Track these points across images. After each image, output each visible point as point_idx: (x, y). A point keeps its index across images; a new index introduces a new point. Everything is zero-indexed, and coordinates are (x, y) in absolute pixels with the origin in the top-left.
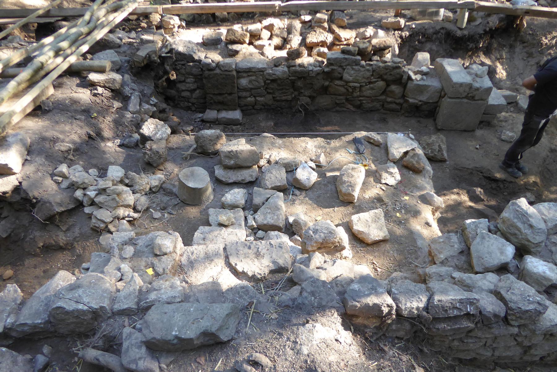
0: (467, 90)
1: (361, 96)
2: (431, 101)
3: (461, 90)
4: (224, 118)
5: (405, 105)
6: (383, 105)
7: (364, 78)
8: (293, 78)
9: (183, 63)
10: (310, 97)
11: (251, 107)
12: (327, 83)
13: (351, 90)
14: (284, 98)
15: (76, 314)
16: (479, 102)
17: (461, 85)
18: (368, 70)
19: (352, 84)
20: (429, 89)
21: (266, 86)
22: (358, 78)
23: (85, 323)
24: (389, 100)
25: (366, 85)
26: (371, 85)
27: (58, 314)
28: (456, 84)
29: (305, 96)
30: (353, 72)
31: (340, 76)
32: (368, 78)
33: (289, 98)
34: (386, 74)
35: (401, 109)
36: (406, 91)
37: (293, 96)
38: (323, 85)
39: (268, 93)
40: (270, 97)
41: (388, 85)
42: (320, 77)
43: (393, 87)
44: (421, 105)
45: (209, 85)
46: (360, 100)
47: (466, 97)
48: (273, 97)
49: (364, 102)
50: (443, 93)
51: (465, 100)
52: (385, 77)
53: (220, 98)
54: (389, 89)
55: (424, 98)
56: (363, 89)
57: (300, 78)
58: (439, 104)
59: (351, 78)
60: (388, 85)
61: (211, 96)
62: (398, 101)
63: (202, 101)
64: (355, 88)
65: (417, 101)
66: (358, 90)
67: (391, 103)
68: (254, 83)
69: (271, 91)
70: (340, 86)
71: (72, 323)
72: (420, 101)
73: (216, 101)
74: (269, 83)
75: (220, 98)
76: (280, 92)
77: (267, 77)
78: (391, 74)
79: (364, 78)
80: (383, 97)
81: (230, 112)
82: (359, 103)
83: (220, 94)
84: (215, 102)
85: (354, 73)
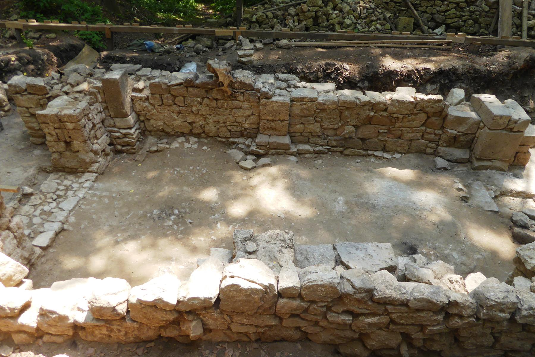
1: (402, 127)
2: (469, 132)
3: (501, 122)
4: (275, 142)
5: (444, 136)
7: (407, 110)
8: (341, 108)
9: (242, 91)
10: (354, 126)
11: (299, 134)
12: (372, 114)
13: (394, 121)
14: (331, 126)
15: (249, 292)
16: (517, 133)
19: (395, 115)
21: (316, 115)
22: (401, 109)
23: (253, 302)
24: (429, 130)
25: (409, 116)
27: (230, 291)
28: (496, 116)
29: (351, 125)
31: (385, 107)
32: (410, 111)
33: (336, 126)
34: (428, 107)
35: (439, 139)
36: (445, 123)
37: (340, 124)
38: (369, 115)
39: (316, 121)
40: (318, 125)
41: (428, 118)
43: (433, 119)
44: (460, 135)
45: (265, 112)
48: (321, 126)
49: (405, 132)
50: (482, 124)
51: (504, 132)
52: (427, 110)
53: (273, 124)
54: (429, 120)
55: (463, 129)
56: (406, 120)
57: (347, 109)
58: (477, 135)
60: (428, 118)
61: (265, 121)
62: (436, 132)
63: (254, 126)
66: (400, 120)
67: (430, 133)
68: (305, 111)
69: (320, 119)
70: (385, 116)
71: (240, 301)
73: (269, 127)
74: (318, 113)
75: (273, 124)
76: (328, 121)
77: (318, 107)
78: (433, 107)
79: (407, 110)
80: (424, 128)
81: (281, 137)
82: (400, 132)
83: (273, 121)
84: (268, 128)
85: (398, 105)
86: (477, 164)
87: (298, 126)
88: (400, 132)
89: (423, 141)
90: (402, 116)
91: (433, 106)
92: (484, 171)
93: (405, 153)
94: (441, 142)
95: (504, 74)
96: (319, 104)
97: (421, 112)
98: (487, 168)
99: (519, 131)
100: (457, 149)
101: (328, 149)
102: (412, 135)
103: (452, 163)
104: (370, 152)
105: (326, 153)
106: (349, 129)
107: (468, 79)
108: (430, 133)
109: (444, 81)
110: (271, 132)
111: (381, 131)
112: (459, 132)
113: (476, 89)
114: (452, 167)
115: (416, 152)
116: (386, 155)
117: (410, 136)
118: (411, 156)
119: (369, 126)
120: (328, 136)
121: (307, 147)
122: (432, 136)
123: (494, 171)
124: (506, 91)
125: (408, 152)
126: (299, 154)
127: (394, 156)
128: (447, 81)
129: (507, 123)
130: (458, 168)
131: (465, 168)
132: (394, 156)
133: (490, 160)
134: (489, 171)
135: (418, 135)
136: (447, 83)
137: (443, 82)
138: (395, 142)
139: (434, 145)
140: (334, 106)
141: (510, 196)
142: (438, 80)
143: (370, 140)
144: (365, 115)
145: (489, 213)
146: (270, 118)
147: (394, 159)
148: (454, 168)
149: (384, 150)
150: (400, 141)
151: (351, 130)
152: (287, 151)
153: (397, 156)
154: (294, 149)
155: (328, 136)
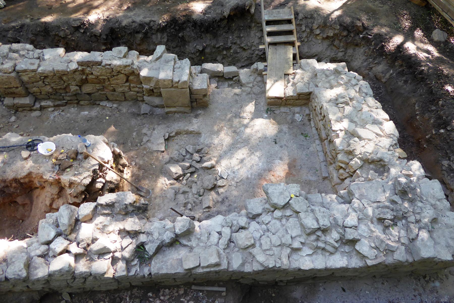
0: (170, 82)
3: (166, 83)
6: (130, 89)
18: (108, 68)
20: (154, 79)
26: (116, 77)
30: (98, 70)
32: (110, 73)
33: (62, 87)
34: (122, 70)
40: (48, 87)
42: (77, 73)
51: (173, 89)
53: (11, 90)
59: (99, 74)
62: (138, 86)
64: (104, 79)
66: (107, 80)
67: (134, 87)
81: (23, 99)
82: (112, 88)
87: (34, 89)
89: (132, 93)
90: (106, 78)
94: (145, 93)
95: (217, 21)
96: (40, 73)
101: (66, 103)
102: (122, 89)
105: (65, 105)
106: (73, 88)
108: (134, 87)
110: (14, 96)
111: (98, 88)
115: (132, 100)
116: (108, 104)
117: (121, 89)
119: (87, 84)
120: (61, 94)
121: (49, 103)
122: (137, 89)
124: (224, 34)
126: (42, 108)
133: (175, 107)
135: (126, 89)
138: (112, 95)
139: (141, 95)
140: (52, 74)
143: (94, 94)
144: (78, 78)
146: (6, 87)
149: (108, 99)
150: (116, 93)
151: (75, 89)
152: (32, 108)
154: (37, 106)
155: (61, 94)
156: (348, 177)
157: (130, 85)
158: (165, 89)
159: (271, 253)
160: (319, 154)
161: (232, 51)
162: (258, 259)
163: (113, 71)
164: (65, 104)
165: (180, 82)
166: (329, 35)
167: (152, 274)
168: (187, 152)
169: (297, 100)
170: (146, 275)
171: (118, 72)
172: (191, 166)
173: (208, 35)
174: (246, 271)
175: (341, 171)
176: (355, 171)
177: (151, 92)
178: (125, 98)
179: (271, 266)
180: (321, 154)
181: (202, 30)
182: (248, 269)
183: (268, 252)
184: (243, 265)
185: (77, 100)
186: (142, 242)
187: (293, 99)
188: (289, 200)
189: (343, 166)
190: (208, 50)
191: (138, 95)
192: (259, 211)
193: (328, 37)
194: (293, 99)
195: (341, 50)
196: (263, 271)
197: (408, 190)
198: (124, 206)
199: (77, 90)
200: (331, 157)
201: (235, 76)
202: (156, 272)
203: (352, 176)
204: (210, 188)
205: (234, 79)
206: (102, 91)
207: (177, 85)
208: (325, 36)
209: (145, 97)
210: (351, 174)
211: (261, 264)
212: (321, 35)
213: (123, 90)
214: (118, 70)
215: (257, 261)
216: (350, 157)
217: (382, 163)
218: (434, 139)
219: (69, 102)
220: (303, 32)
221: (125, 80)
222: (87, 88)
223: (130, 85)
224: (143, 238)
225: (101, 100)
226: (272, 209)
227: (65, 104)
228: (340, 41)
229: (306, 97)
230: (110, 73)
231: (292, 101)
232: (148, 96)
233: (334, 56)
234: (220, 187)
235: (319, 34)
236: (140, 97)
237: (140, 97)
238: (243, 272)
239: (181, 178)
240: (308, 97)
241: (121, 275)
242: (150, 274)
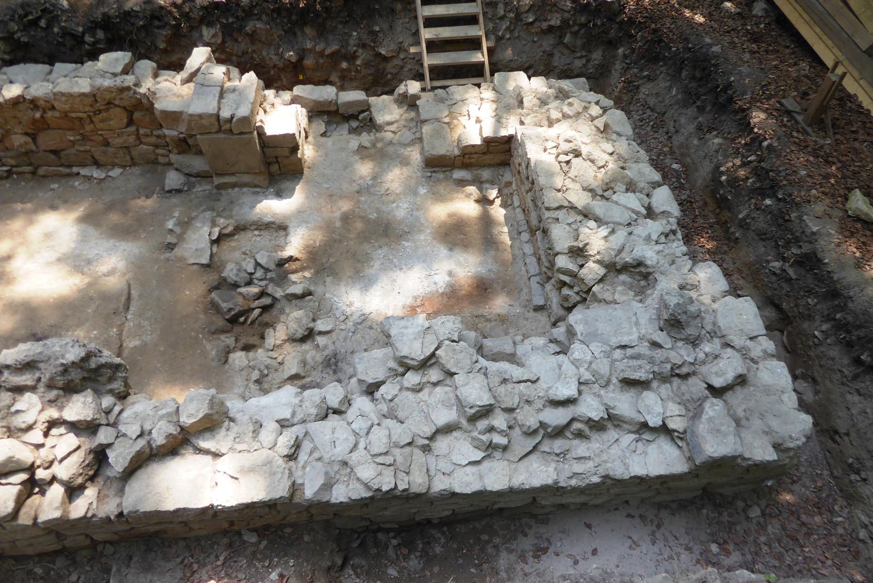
0: (213, 120)
16: (243, 136)
17: (200, 116)
42: (22, 107)
46: (101, 135)
47: (219, 131)
51: (222, 136)
59: (67, 107)
62: (155, 133)
64: (80, 119)
65: (176, 133)
66: (88, 121)
67: (147, 136)
72: (182, 133)
78: (121, 99)
80: (132, 129)
86: (217, 181)
88: (101, 138)
89: (145, 147)
90: (85, 115)
91: (122, 96)
92: (230, 190)
93: (130, 166)
97: (111, 106)
98: (234, 185)
99: (242, 133)
100: (196, 156)
103: (193, 179)
104: (75, 170)
107: (267, 15)
108: (147, 136)
109: (227, 20)
112: (182, 133)
113: (286, 28)
114: (191, 186)
115: (147, 163)
117: (118, 141)
118: (136, 170)
119: (49, 131)
122: (153, 140)
123: (245, 190)
124: (340, 26)
125: (134, 164)
127: (110, 174)
128: (231, 20)
129: (216, 123)
130: (201, 185)
131: (208, 187)
132: (110, 174)
133: (233, 174)
134: (236, 189)
135: (132, 140)
136: (233, 23)
137: (224, 21)
138: (104, 152)
139: (164, 151)
141: (256, 229)
142: (214, 19)
143: (65, 152)
145: (195, 267)
147: (110, 179)
148: (194, 187)
149: (97, 164)
150: (111, 150)
153: (116, 172)
156: (578, 302)
157: (138, 130)
158: (206, 136)
159: (389, 460)
160: (528, 261)
161: (358, 62)
162: (359, 475)
163: (96, 101)
164: (5, 175)
165: (234, 119)
166: (552, 23)
167: (125, 512)
168: (258, 264)
169: (484, 153)
170: (112, 518)
171: (108, 103)
172: (262, 294)
173: (308, 30)
174: (333, 501)
175: (566, 291)
176: (590, 289)
177: (185, 145)
178: (132, 159)
179: (385, 488)
180: (532, 261)
181: (294, 18)
182: (340, 494)
183: (380, 460)
184: (328, 486)
185: (30, 164)
186: (101, 445)
187: (476, 153)
188: (436, 349)
189: (566, 279)
190: (309, 62)
191: (159, 151)
192: (380, 377)
193: (551, 29)
194: (476, 153)
195: (579, 55)
196: (372, 498)
197: (683, 318)
198: (60, 369)
199: (26, 143)
200: (547, 264)
201: (363, 111)
202: (130, 508)
203: (585, 299)
204: (299, 335)
205: (361, 117)
206: (81, 145)
207: (228, 126)
208: (545, 25)
209: (171, 156)
210: (584, 296)
211: (367, 486)
212: (537, 24)
213: (125, 142)
214: (108, 97)
215: (358, 479)
216: (580, 261)
217: (642, 269)
218: (753, 219)
219: (14, 169)
220: (502, 18)
221: (125, 120)
222: (47, 140)
223: (138, 130)
224: (104, 436)
225: (83, 165)
226: (401, 370)
227: (5, 175)
228: (575, 34)
229: (502, 146)
230: (91, 106)
231: (475, 156)
232: (179, 154)
233: (565, 68)
234: (321, 333)
235: (532, 23)
236: (162, 155)
237: (162, 155)
238: (328, 504)
239: (242, 319)
240: (507, 146)
241: (50, 518)
242: (121, 514)
